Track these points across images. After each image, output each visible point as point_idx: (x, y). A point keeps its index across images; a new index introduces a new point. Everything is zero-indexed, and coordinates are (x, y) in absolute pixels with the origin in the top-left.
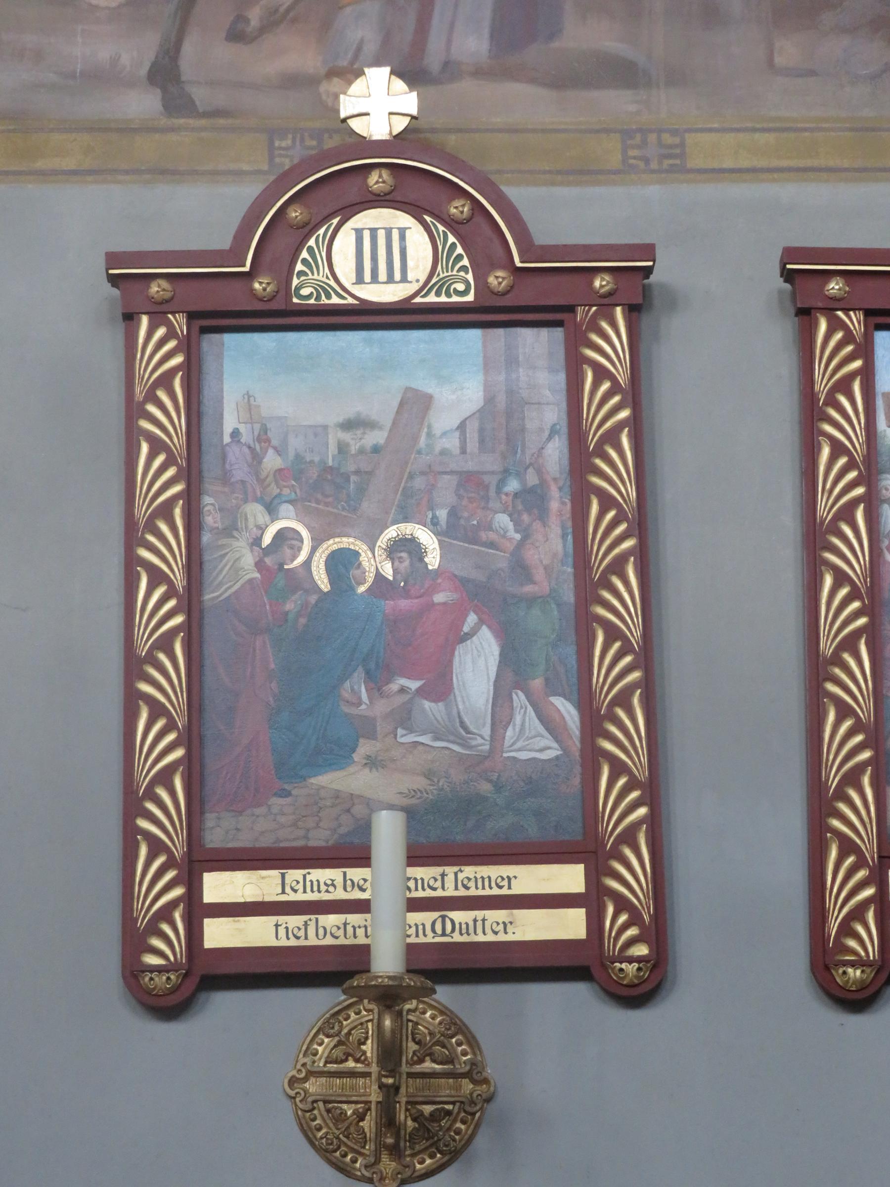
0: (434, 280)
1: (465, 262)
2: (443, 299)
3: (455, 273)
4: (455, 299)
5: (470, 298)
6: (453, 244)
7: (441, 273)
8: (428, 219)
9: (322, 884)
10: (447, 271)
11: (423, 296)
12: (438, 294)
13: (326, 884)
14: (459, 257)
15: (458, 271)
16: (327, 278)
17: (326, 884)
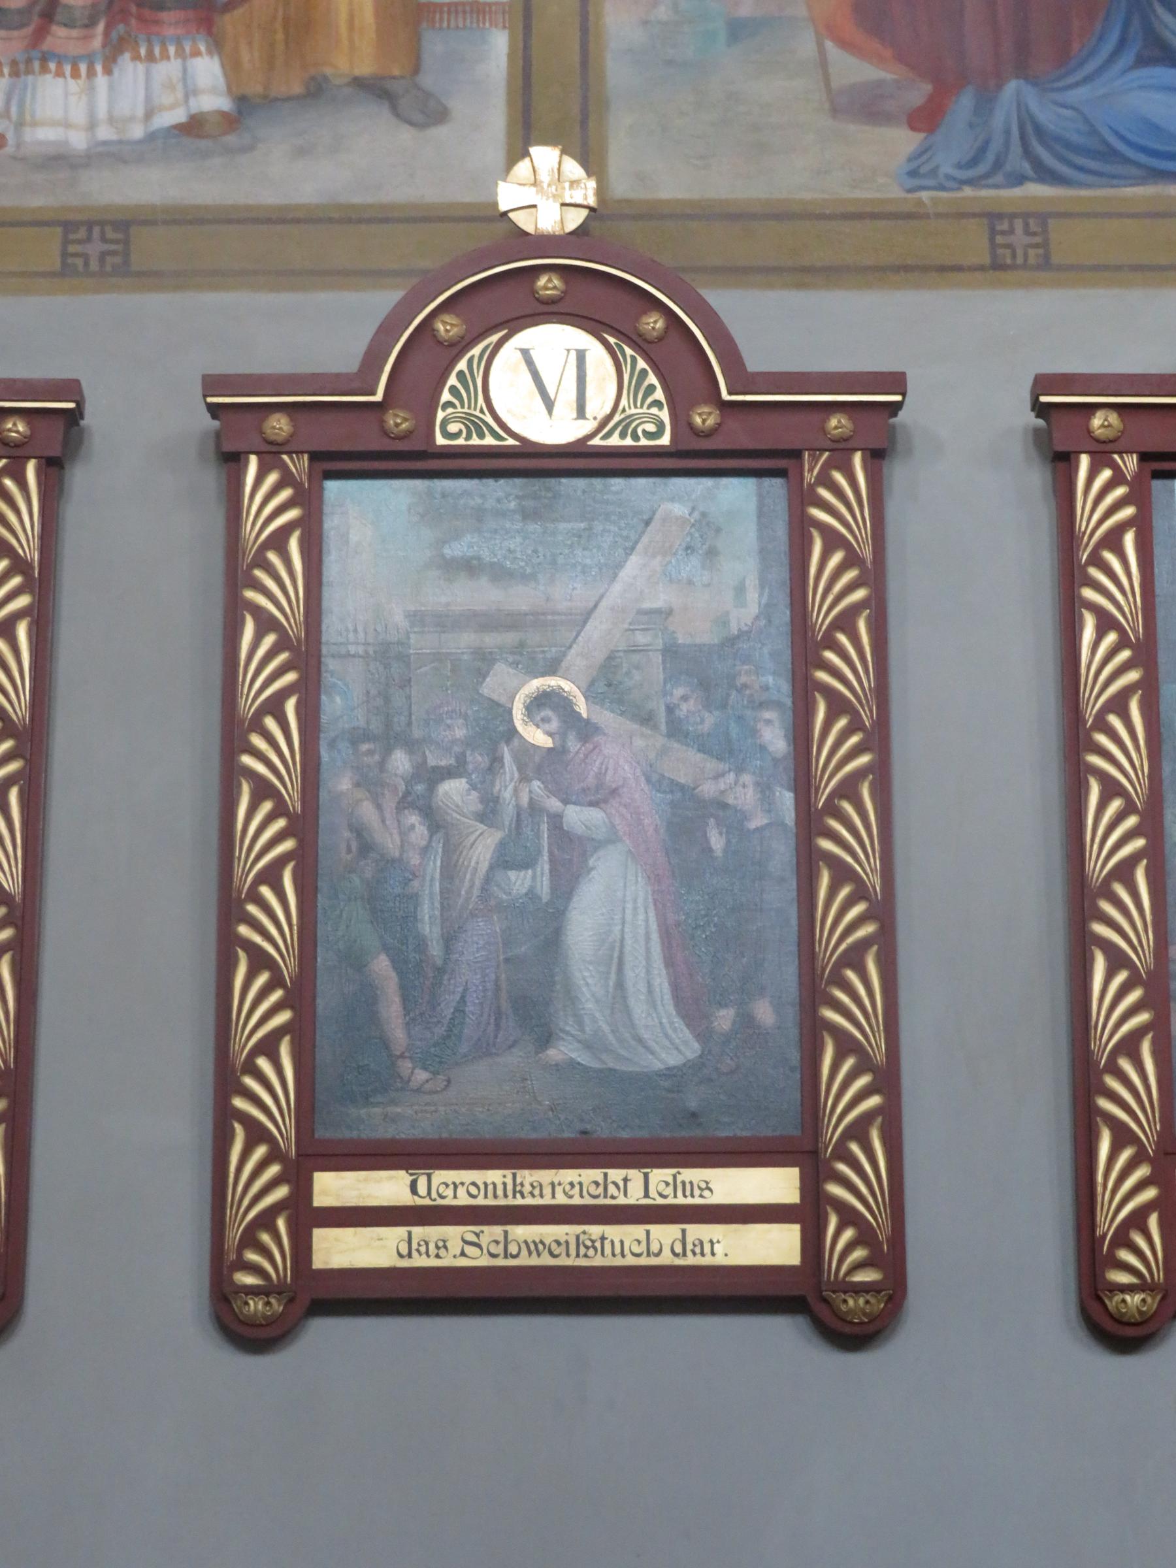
0: (617, 418)
1: (659, 394)
3: (644, 410)
4: (644, 442)
5: (665, 440)
8: (612, 340)
9: (696, 1188)
11: (603, 438)
12: (623, 435)
13: (699, 1188)
14: (651, 389)
16: (482, 411)
17: (699, 1188)
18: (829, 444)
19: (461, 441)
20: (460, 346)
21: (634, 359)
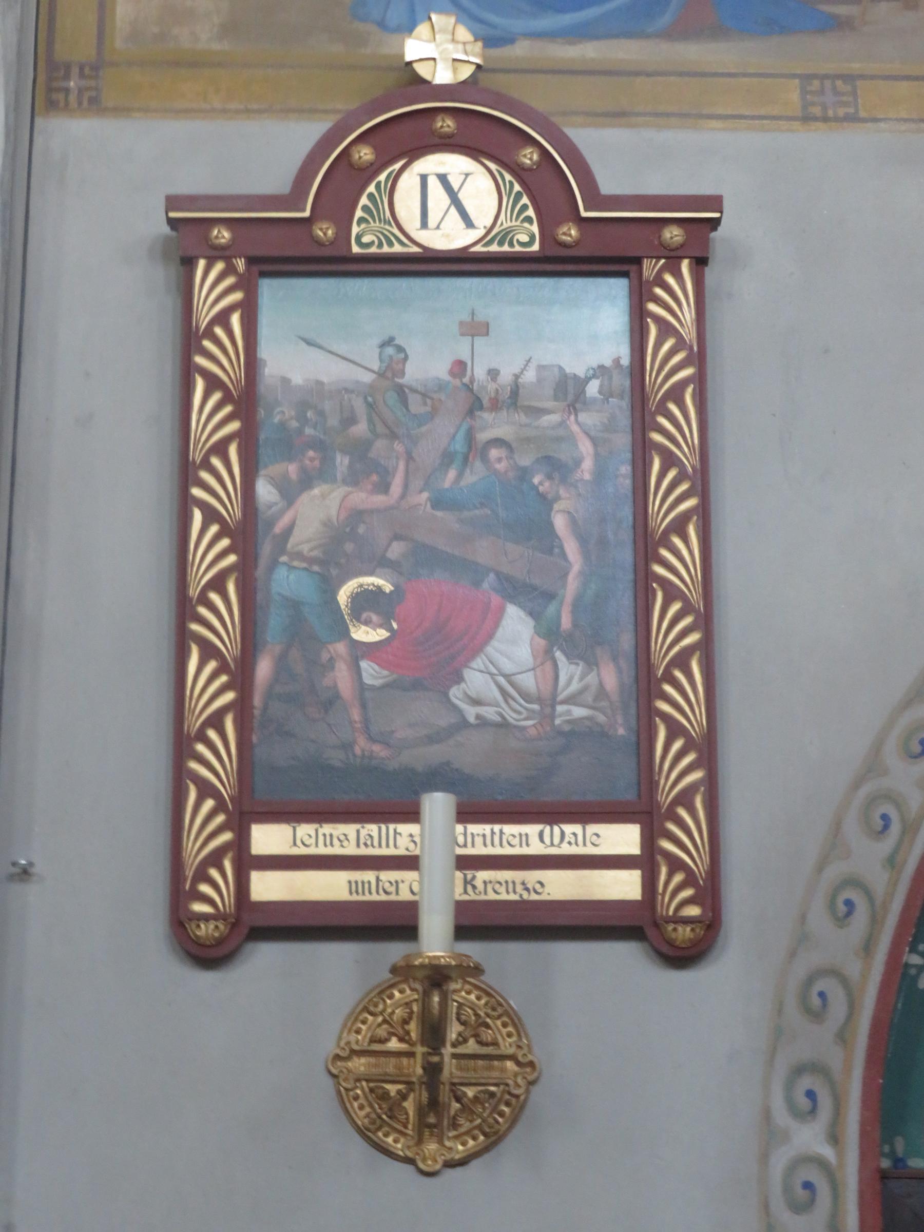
1: (531, 212)
2: (506, 248)
4: (518, 248)
5: (536, 247)
6: (518, 193)
7: (504, 222)
8: (493, 166)
10: (511, 220)
11: (486, 245)
12: (501, 243)
14: (524, 207)
15: (523, 221)
18: (667, 253)
19: (373, 250)
20: (371, 171)
21: (511, 183)
